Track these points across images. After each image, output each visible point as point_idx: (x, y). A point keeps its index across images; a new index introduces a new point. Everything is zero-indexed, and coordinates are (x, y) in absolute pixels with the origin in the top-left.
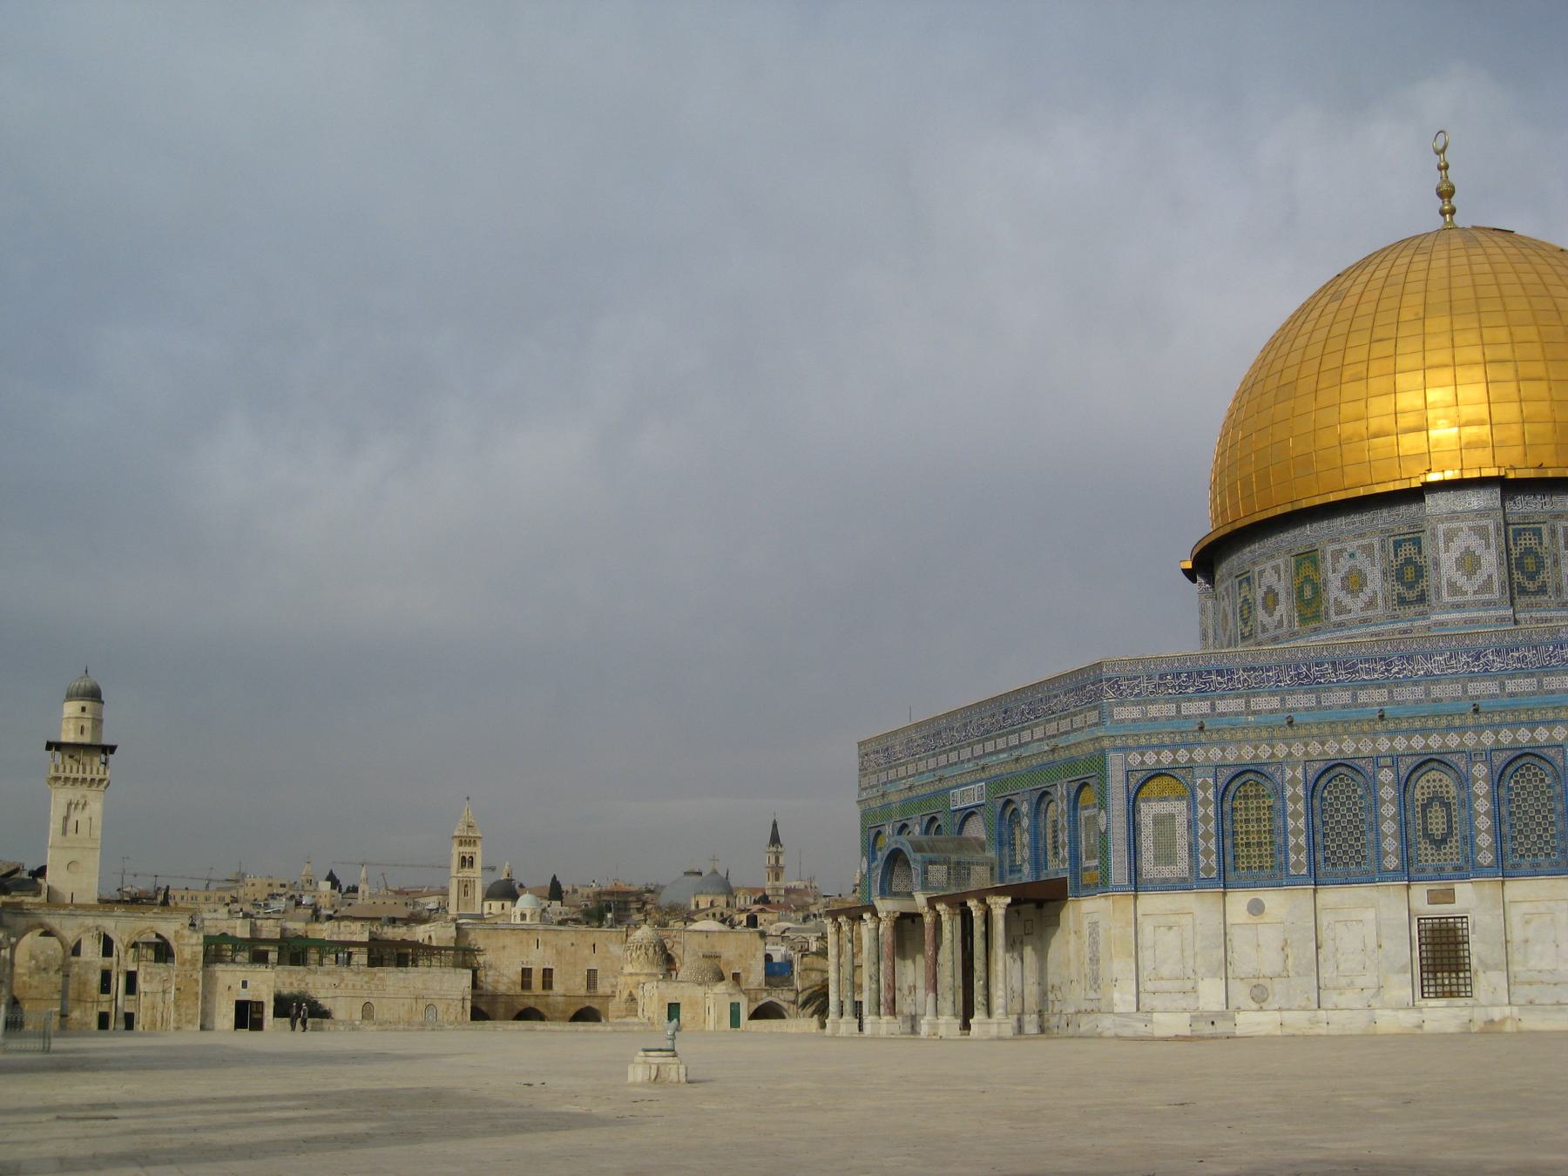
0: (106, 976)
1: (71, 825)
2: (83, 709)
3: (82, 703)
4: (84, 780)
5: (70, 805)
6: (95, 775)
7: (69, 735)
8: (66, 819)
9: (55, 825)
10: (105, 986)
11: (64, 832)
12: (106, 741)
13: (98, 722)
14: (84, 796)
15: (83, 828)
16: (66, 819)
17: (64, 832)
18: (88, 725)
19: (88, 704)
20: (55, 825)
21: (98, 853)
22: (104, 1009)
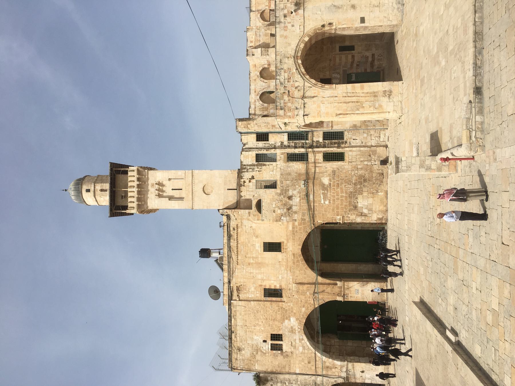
0: (292, 158)
1: (176, 194)
2: (88, 191)
3: (84, 192)
4: (139, 186)
5: (160, 196)
6: (135, 179)
7: (105, 200)
8: (171, 198)
9: (174, 205)
10: (302, 158)
11: (181, 199)
12: (106, 171)
13: (98, 179)
14: (153, 185)
15: (178, 184)
16: (171, 198)
17: (181, 199)
18: (99, 187)
19: (85, 187)
20: (174, 205)
21: (196, 172)
22: (320, 157)
